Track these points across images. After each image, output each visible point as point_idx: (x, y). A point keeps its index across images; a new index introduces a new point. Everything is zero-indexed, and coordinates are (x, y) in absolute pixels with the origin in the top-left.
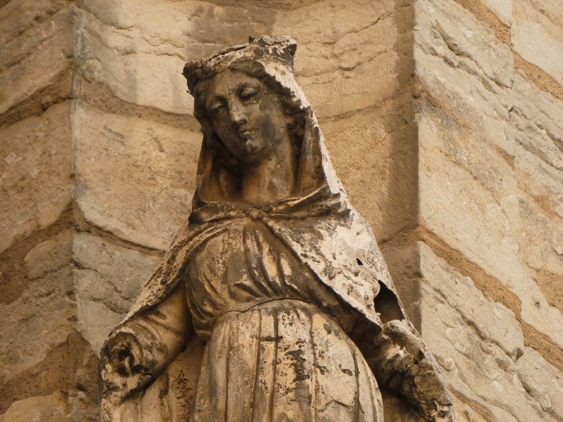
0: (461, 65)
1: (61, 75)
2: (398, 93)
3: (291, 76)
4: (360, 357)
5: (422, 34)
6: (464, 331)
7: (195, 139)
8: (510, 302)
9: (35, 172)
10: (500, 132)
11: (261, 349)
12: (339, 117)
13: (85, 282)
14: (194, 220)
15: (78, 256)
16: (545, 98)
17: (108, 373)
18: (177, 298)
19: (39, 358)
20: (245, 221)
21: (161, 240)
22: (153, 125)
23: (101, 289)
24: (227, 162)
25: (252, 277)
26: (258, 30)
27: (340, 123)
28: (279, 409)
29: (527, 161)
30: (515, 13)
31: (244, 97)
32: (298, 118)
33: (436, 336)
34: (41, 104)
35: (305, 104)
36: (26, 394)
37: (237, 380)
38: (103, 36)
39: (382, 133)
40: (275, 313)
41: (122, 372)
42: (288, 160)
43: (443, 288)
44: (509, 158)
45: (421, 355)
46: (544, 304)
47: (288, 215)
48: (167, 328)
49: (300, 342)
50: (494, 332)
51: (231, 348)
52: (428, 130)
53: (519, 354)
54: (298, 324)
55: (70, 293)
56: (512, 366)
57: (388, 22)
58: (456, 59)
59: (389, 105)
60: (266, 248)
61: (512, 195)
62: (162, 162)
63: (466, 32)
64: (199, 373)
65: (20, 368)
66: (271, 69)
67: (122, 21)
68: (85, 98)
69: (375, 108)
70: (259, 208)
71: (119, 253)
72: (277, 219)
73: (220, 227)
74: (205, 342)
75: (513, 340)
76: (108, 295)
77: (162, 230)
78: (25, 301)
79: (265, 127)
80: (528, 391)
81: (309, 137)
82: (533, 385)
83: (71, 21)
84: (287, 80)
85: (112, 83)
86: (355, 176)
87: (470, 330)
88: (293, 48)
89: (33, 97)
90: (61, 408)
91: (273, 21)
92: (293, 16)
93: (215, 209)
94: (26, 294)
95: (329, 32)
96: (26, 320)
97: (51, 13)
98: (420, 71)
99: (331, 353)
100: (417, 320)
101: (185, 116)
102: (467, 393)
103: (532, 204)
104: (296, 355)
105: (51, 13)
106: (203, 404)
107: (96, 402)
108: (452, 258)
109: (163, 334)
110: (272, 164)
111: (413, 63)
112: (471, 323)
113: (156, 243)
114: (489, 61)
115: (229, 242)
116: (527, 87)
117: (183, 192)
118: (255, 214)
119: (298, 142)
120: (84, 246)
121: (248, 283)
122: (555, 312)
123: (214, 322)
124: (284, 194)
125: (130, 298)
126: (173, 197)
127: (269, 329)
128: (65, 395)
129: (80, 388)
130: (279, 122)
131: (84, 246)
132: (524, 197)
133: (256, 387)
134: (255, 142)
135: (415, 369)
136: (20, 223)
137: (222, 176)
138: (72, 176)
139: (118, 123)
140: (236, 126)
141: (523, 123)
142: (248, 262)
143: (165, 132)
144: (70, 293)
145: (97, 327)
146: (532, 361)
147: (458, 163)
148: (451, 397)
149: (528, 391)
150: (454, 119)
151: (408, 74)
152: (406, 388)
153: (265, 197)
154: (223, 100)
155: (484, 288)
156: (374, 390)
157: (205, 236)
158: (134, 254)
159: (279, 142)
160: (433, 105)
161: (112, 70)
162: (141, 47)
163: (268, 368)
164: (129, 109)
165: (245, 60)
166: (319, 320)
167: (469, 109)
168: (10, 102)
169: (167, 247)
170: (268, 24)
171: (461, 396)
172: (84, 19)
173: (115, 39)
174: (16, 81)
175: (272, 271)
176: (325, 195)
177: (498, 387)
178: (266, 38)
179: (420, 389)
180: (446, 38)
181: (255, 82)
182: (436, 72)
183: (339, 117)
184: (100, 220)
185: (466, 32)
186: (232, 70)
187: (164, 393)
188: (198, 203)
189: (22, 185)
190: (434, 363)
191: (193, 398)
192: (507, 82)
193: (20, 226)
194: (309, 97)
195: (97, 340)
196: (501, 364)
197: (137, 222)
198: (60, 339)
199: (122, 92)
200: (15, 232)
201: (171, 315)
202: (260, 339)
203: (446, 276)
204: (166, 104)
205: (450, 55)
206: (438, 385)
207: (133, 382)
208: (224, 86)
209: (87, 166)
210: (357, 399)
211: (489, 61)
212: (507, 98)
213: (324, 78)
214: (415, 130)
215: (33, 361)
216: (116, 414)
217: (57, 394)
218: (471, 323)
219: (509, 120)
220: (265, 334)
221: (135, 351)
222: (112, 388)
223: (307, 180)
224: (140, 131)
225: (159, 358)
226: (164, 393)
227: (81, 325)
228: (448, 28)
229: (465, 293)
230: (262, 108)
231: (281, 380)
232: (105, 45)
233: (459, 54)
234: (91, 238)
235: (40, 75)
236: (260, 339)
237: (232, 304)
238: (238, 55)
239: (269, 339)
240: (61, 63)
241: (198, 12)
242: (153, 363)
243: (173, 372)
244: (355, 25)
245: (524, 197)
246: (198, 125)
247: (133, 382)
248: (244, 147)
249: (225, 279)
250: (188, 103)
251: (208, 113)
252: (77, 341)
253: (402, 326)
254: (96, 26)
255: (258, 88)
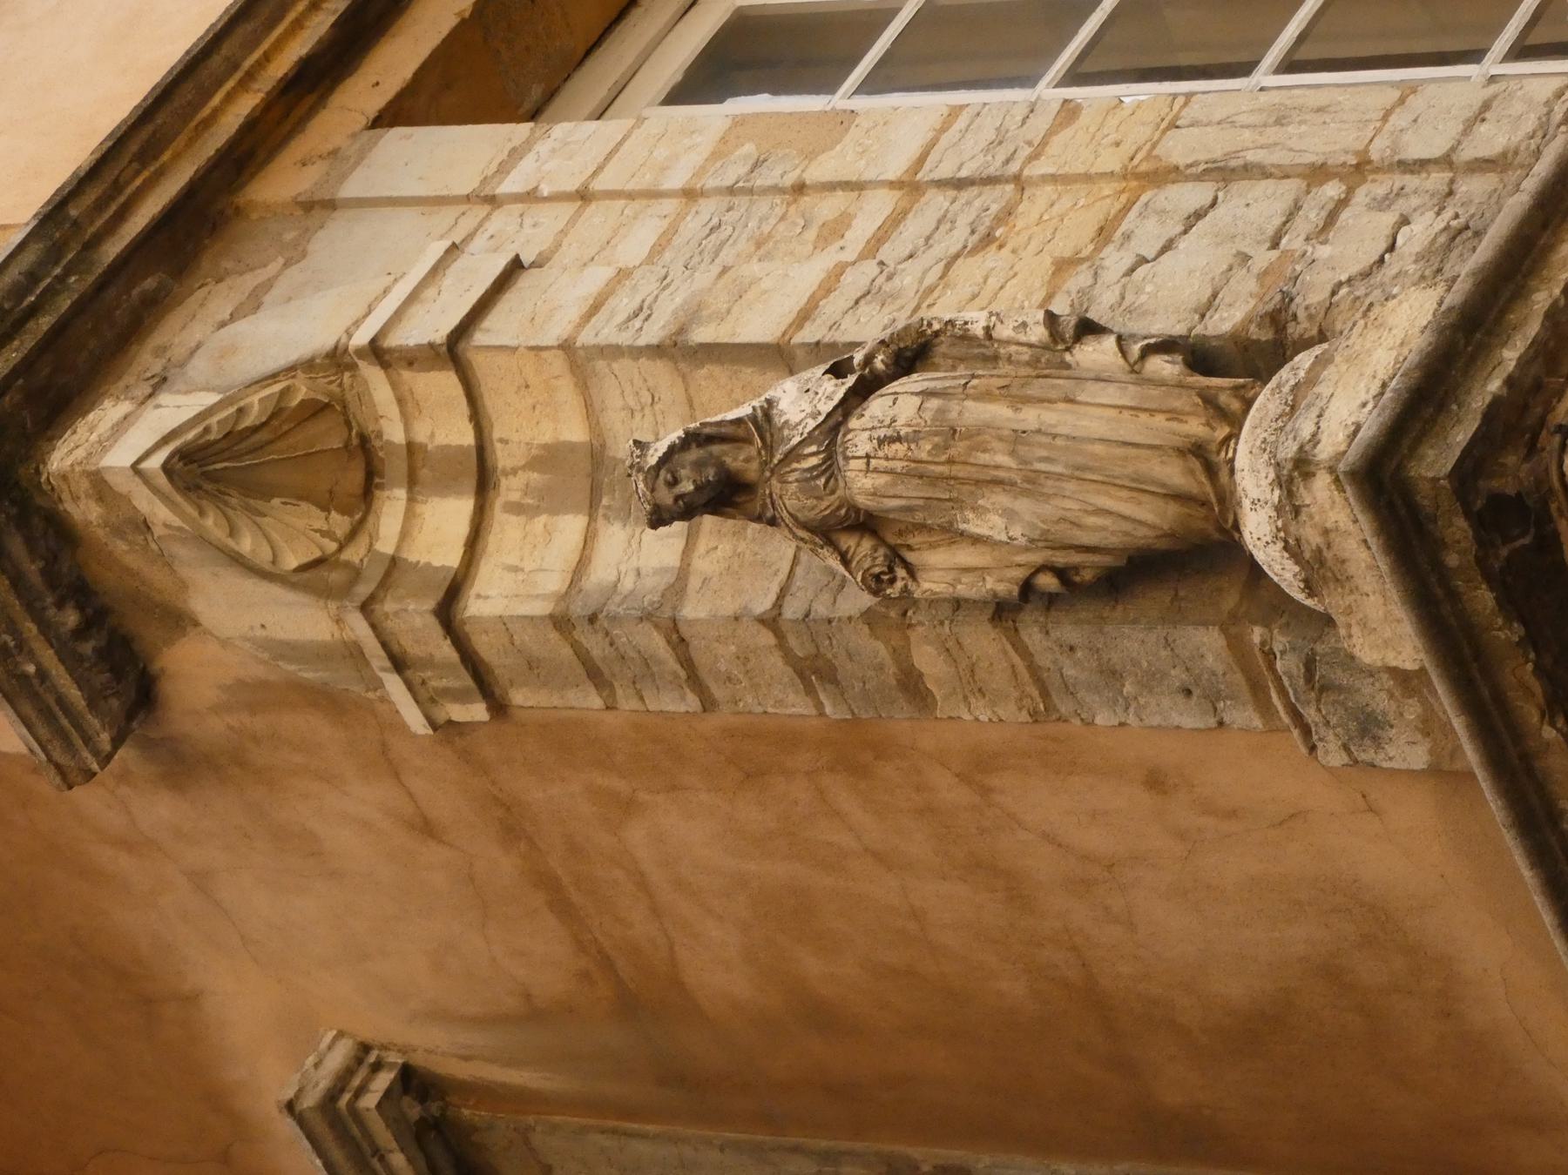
0: (650, 308)
1: (656, 626)
2: (672, 358)
3: (658, 444)
4: (883, 391)
5: (624, 339)
6: (863, 307)
7: (708, 521)
8: (839, 270)
9: (733, 648)
10: (704, 277)
11: (876, 470)
12: (691, 406)
13: (821, 609)
14: (772, 522)
15: (800, 616)
16: (677, 241)
17: (894, 591)
18: (834, 537)
19: (880, 646)
20: (774, 482)
21: (789, 549)
22: (696, 554)
23: (826, 597)
24: (726, 495)
25: (818, 477)
26: (620, 471)
27: (696, 405)
28: (924, 456)
29: (727, 256)
30: (609, 265)
31: (675, 482)
32: (692, 439)
33: (868, 329)
34: (679, 642)
35: (681, 433)
36: (909, 656)
37: (900, 490)
38: (625, 592)
39: (703, 372)
40: (847, 459)
41: (892, 581)
42: (725, 447)
43: (829, 323)
44: (725, 270)
45: (882, 342)
46: (841, 243)
47: (769, 448)
48: (858, 545)
49: (871, 439)
50: (864, 283)
51: (874, 494)
52: (702, 334)
53: (882, 263)
54: (856, 441)
55: (830, 622)
56: (891, 269)
57: (615, 366)
58: (646, 312)
59: (682, 365)
60: (795, 465)
61: (755, 268)
62: (725, 548)
63: (623, 303)
64: (894, 520)
65: (888, 661)
66: (652, 460)
67: (613, 578)
68: (674, 608)
69: (684, 377)
70: (763, 471)
71: (798, 582)
72: (772, 456)
73: (778, 502)
74: (870, 515)
75: (871, 268)
76: (833, 592)
77: (780, 548)
78: (835, 657)
79: (699, 465)
80: (911, 256)
81: (707, 430)
82: (907, 253)
83: (614, 619)
84: (661, 448)
85: (662, 587)
86: (738, 394)
87: (862, 302)
88: (635, 442)
89: (674, 649)
90: (920, 629)
91: (614, 458)
92: (609, 442)
93: (764, 506)
94: (830, 656)
95: (623, 414)
96: (850, 656)
97: (607, 634)
98: (655, 341)
99: (879, 414)
100: (854, 345)
101: (690, 528)
102: (913, 305)
103: (762, 251)
104: (881, 442)
105: (607, 634)
106: (919, 517)
107: (916, 602)
108: (805, 316)
109: (863, 548)
110: (728, 460)
111: (648, 347)
112: (857, 302)
113: (790, 553)
114: (647, 285)
115: (790, 496)
116: (668, 255)
117: (749, 531)
118: (768, 474)
119: (710, 439)
120: (792, 610)
121: (823, 480)
122: (847, 235)
123: (854, 509)
124: (753, 451)
125: (833, 574)
126: (754, 539)
127: (861, 464)
128: (910, 626)
129: (905, 614)
130: (694, 454)
131: (792, 610)
132: (755, 259)
133: (909, 474)
134: (711, 473)
135: (893, 347)
136: (773, 660)
137: (738, 500)
138: (736, 619)
139: (694, 582)
140: (698, 488)
141: (696, 259)
142: (806, 480)
143: (702, 545)
144: (830, 622)
145: (858, 600)
146: (888, 252)
147: (729, 311)
148: (915, 319)
149: (911, 256)
150: (693, 314)
151: (657, 351)
152: (908, 354)
153: (755, 465)
154: (677, 498)
155: (829, 291)
156: (995, 372)
157: (785, 514)
158: (799, 571)
159: (711, 454)
160: (682, 330)
161: (653, 586)
162: (634, 563)
163: (891, 464)
164: (683, 573)
165: (645, 480)
166: (853, 423)
167: (685, 302)
168: (677, 667)
169: (794, 545)
170: (617, 462)
171: (917, 308)
172: (612, 607)
173: (628, 584)
174: (660, 662)
175: (814, 461)
176: (753, 418)
177: (908, 280)
178: (628, 463)
179: (909, 343)
180: (629, 319)
181: (663, 473)
182: (656, 328)
183: (691, 406)
184: (772, 597)
185: (623, 303)
186: (653, 490)
187: (910, 548)
188: (758, 519)
189: (743, 658)
190: (889, 331)
191: (914, 525)
192: (664, 271)
193: (775, 661)
194: (674, 430)
195: (867, 600)
196: (890, 278)
197: (774, 568)
198: (866, 628)
199: (670, 578)
200: (780, 663)
201: (848, 542)
202: (868, 471)
203: (819, 321)
204: (679, 544)
205: (642, 316)
206: (907, 328)
207: (901, 572)
208: (666, 497)
209: (728, 607)
210: (917, 394)
211: (647, 285)
212: (677, 271)
213: (660, 418)
214: (702, 345)
215: (882, 651)
216: (926, 586)
217: (909, 632)
218: (857, 302)
219: (694, 269)
220: (864, 467)
221: (877, 570)
222: (905, 589)
223: (741, 432)
224: (702, 564)
225: (882, 551)
226: (910, 548)
227: (855, 612)
228: (620, 317)
229: (833, 307)
230: (683, 467)
231: (901, 455)
232: (632, 592)
233: (641, 309)
234: (785, 605)
235: (657, 644)
236: (868, 471)
237: (839, 493)
238: (641, 485)
239: (868, 464)
240: (647, 626)
241: (606, 517)
242: (886, 556)
243: (892, 540)
244: (618, 392)
245: (755, 259)
246: (696, 519)
247: (901, 572)
248: (715, 482)
249: (819, 498)
250: (679, 526)
251: (688, 510)
252: (868, 616)
253: (858, 357)
254: (617, 599)
255: (669, 471)
